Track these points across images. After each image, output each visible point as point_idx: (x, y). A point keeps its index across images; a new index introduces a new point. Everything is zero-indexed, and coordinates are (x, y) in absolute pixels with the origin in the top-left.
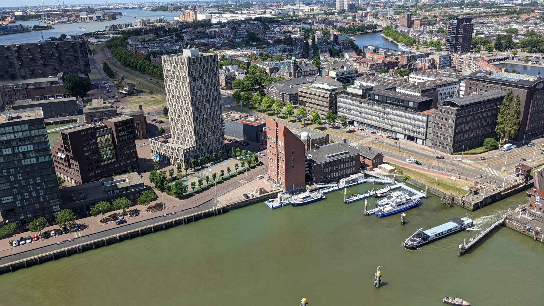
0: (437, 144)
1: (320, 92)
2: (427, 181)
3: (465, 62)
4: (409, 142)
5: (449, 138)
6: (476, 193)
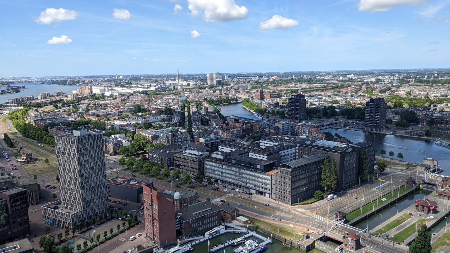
0: (281, 198)
1: (191, 157)
2: (272, 229)
3: (301, 128)
4: (259, 196)
5: (288, 193)
6: (308, 237)
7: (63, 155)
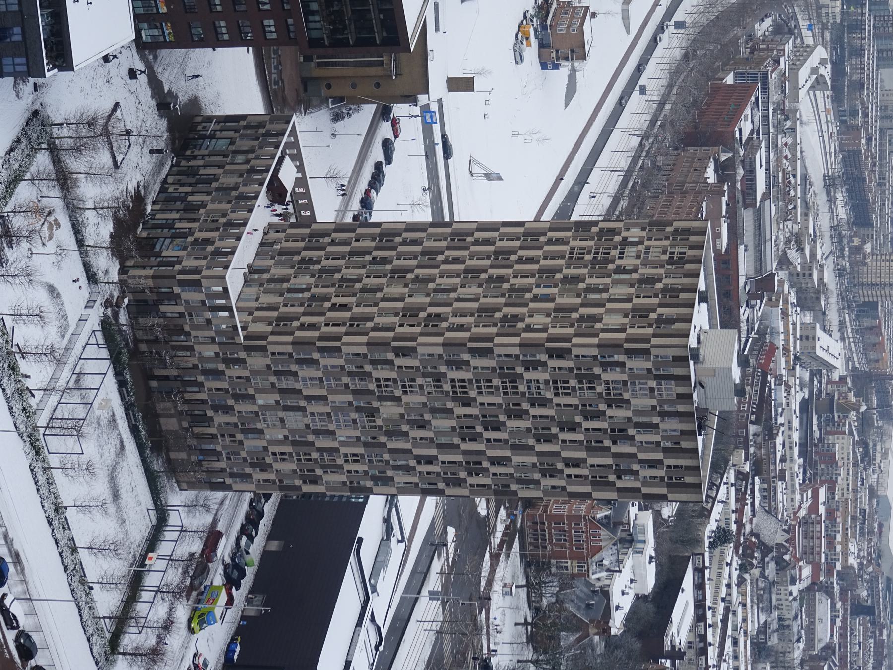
7: (588, 257)
